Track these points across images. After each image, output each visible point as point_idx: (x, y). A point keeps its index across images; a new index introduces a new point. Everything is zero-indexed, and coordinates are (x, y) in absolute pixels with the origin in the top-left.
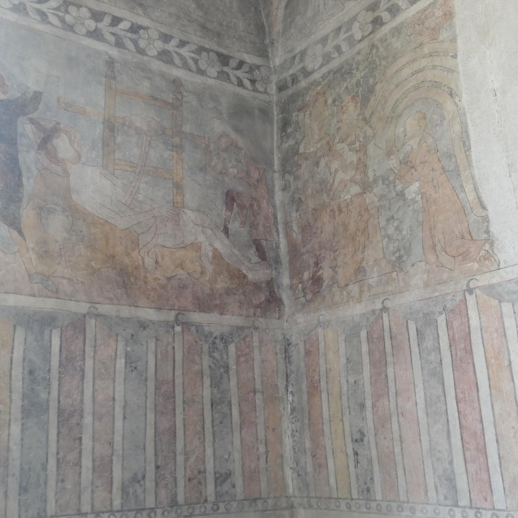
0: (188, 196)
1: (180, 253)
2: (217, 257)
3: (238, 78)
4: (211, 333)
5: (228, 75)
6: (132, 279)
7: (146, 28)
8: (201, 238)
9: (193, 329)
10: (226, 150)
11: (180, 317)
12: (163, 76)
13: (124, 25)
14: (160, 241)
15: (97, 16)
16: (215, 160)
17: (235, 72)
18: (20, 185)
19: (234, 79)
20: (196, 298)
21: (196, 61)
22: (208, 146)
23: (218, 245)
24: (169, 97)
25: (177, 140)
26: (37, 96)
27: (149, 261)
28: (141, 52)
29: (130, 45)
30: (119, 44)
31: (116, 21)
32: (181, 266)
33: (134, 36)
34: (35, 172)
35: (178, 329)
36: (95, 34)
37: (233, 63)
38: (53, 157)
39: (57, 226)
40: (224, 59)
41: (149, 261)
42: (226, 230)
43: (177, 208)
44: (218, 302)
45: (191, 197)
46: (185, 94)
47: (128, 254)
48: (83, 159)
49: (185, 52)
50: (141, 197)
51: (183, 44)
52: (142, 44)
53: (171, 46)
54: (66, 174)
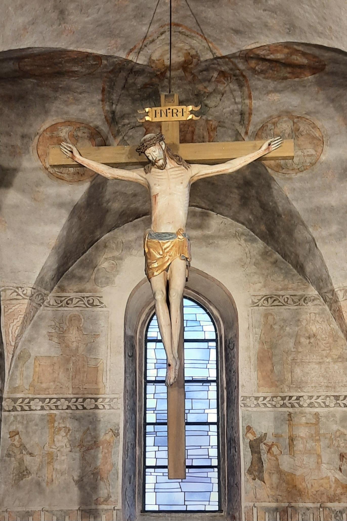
0: (323, 459)
1: (322, 481)
2: (337, 480)
3: (344, 404)
4: (335, 510)
5: (339, 404)
6: (303, 493)
7: (302, 397)
8: (330, 474)
9: (328, 509)
10: (339, 437)
11: (322, 505)
12: (310, 413)
13: (294, 398)
14: (313, 477)
15: (283, 398)
16: (334, 442)
17: (342, 402)
18: (263, 467)
19: (342, 405)
20: (328, 497)
21: (324, 403)
22: (331, 437)
23: (337, 476)
24: (314, 421)
25: (317, 438)
26: (266, 434)
27: (309, 486)
28: (301, 406)
29: (296, 405)
30: (293, 406)
31: (291, 397)
32: (322, 486)
33: (298, 401)
34: (267, 461)
35: (321, 509)
36: (284, 405)
37: (341, 398)
38: (272, 454)
39: (275, 478)
40: (337, 398)
41: (309, 486)
42: (340, 470)
43: (319, 464)
44: (337, 498)
45: (325, 458)
46: (320, 418)
47: (301, 484)
48: (283, 453)
49: (319, 400)
50: (304, 463)
51: (318, 397)
52: (301, 403)
53: (313, 400)
54: (277, 459)
